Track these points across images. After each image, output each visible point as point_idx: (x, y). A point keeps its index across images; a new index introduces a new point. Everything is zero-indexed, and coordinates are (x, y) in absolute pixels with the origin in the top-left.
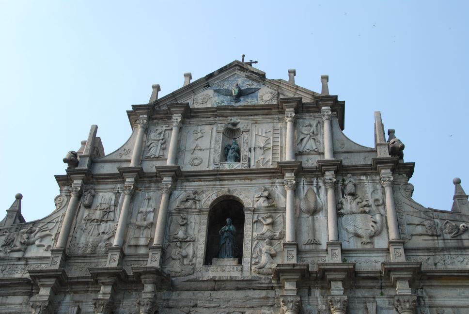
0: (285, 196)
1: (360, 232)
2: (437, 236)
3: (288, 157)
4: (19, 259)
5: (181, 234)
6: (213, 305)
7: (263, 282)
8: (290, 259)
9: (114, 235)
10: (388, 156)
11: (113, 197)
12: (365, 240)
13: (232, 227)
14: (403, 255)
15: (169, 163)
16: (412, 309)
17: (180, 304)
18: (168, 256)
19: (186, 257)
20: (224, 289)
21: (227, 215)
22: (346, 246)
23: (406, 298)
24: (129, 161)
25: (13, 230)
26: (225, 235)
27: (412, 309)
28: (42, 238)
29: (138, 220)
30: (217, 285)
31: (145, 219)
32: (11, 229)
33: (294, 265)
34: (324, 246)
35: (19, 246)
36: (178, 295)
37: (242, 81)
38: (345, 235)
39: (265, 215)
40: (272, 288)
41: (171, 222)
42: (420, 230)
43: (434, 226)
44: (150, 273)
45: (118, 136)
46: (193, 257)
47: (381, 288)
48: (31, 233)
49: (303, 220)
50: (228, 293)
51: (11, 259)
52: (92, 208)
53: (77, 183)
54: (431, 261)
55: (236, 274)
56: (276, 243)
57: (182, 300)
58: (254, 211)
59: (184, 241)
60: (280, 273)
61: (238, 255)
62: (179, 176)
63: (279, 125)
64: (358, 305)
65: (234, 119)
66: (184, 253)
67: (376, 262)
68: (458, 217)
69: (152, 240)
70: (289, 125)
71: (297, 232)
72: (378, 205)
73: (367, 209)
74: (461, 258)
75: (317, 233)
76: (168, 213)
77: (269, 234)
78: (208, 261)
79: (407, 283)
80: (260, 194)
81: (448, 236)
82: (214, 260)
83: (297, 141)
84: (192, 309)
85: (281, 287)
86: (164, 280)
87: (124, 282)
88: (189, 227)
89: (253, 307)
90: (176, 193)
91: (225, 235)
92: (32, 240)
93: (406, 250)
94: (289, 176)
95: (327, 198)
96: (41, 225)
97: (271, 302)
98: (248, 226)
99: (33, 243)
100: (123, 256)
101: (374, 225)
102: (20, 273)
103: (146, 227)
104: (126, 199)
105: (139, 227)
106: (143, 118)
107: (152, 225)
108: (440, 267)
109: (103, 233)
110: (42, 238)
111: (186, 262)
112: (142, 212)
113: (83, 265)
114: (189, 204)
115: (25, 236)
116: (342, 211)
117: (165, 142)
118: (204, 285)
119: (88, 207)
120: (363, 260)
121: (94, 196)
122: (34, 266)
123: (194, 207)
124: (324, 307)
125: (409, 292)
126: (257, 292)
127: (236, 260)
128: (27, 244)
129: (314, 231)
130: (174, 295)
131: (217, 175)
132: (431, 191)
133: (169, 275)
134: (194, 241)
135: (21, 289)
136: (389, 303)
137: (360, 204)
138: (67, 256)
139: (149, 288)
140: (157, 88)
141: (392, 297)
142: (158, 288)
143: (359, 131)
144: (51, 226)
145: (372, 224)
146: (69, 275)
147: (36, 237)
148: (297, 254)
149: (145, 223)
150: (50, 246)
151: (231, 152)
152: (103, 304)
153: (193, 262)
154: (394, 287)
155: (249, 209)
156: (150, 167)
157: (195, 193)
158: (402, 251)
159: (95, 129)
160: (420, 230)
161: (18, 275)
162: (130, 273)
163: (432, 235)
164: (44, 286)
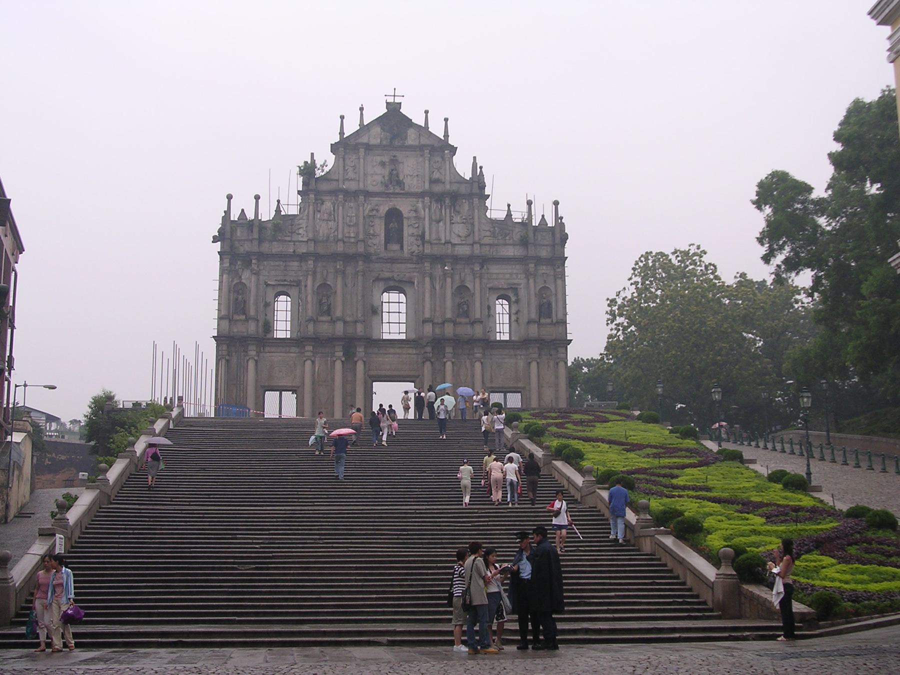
3: (427, 186)
5: (372, 232)
8: (428, 250)
9: (337, 230)
10: (478, 192)
15: (361, 186)
22: (454, 241)
24: (338, 180)
30: (393, 261)
34: (443, 241)
42: (488, 234)
45: (326, 160)
58: (408, 218)
60: (421, 258)
61: (400, 241)
62: (368, 194)
63: (421, 159)
65: (394, 153)
66: (374, 242)
69: (357, 234)
70: (427, 162)
78: (386, 248)
86: (367, 257)
93: (481, 245)
94: (427, 199)
95: (446, 213)
98: (405, 228)
104: (341, 208)
105: (349, 226)
114: (374, 212)
128: (292, 233)
129: (438, 232)
130: (371, 265)
132: (496, 210)
139: (361, 263)
142: (364, 262)
154: (473, 264)
159: (312, 154)
160: (488, 234)
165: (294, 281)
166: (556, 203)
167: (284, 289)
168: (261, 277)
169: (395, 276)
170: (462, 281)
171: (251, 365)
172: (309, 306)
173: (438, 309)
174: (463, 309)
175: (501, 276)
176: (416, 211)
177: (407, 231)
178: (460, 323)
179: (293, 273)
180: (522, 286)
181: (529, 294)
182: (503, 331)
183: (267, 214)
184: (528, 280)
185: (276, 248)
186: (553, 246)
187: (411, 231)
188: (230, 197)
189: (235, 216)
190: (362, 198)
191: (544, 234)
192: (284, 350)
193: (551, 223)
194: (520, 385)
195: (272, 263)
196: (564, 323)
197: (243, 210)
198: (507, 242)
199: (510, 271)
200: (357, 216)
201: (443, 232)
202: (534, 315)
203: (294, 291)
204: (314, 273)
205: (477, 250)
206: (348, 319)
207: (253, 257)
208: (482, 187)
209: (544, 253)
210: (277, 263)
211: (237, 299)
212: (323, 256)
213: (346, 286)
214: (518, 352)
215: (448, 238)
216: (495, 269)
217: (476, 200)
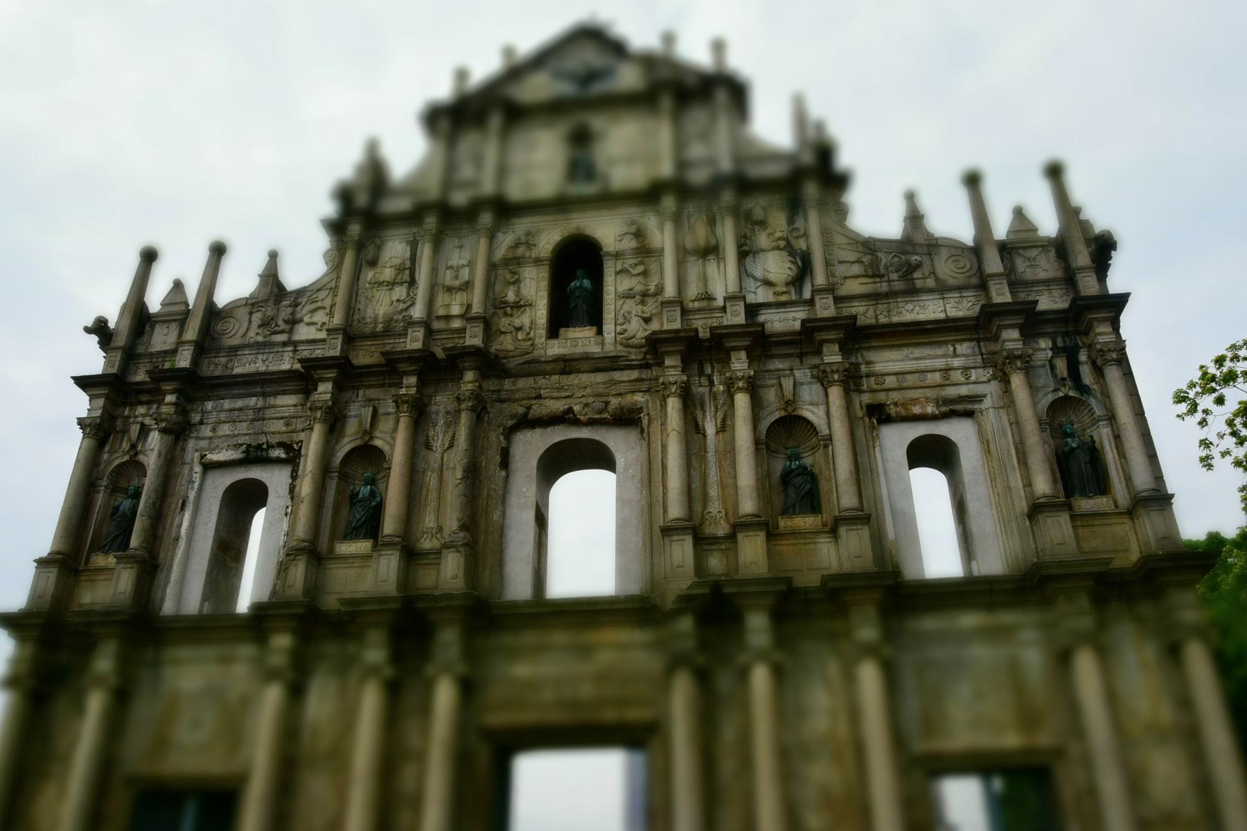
0: (662, 231)
1: (772, 277)
2: (881, 276)
4: (285, 344)
5: (511, 296)
6: (564, 394)
7: (633, 357)
8: (671, 322)
11: (408, 249)
12: (779, 289)
13: (586, 283)
14: (833, 307)
16: (842, 381)
17: (517, 396)
18: (494, 329)
19: (519, 329)
20: (579, 371)
21: (578, 264)
22: (751, 299)
23: (835, 368)
25: (270, 303)
26: (577, 293)
27: (842, 381)
28: (313, 311)
29: (448, 278)
30: (567, 365)
31: (457, 277)
32: (266, 301)
33: (677, 331)
34: (720, 302)
35: (282, 326)
36: (514, 384)
37: (590, 57)
38: (750, 284)
39: (632, 261)
40: (647, 366)
41: (496, 278)
42: (856, 269)
43: (875, 263)
44: (470, 354)
45: (408, 152)
46: (531, 329)
47: (801, 356)
48: (296, 305)
49: (689, 264)
50: (585, 378)
51: (273, 344)
52: (381, 262)
53: (355, 229)
54: (870, 313)
55: (595, 349)
56: (650, 301)
57: (518, 390)
58: (617, 255)
59: (518, 306)
60: (656, 345)
61: (596, 320)
62: (505, 210)
64: (769, 382)
66: (517, 322)
67: (794, 319)
68: (909, 248)
69: (469, 307)
71: (681, 283)
72: (798, 237)
73: (782, 244)
74: (910, 307)
75: (710, 282)
76: (492, 267)
77: (639, 288)
79: (836, 348)
80: (625, 229)
81: (894, 276)
82: (562, 331)
83: (680, 145)
84: (533, 402)
85: (661, 364)
86: (490, 364)
87: (436, 367)
88: (522, 285)
89: (620, 394)
90: (500, 236)
91: (577, 293)
92: (298, 316)
93: (838, 300)
94: (669, 202)
96: (308, 294)
97: (645, 386)
99: (301, 321)
100: (430, 332)
101: (792, 266)
102: (286, 363)
103: (460, 289)
105: (449, 290)
106: (444, 124)
107: (467, 286)
108: (883, 320)
109: (398, 301)
110: (313, 311)
111: (520, 336)
112: (451, 267)
113: (373, 349)
114: (521, 251)
115: (289, 310)
116: (746, 248)
117: (478, 161)
118: (548, 368)
119: (373, 263)
120: (776, 317)
121: (379, 247)
122: (305, 352)
123: (527, 255)
124: (721, 388)
125: (838, 358)
126: (627, 373)
127: (595, 329)
128: (293, 322)
129: (705, 280)
130: (507, 384)
131: (559, 205)
132: (874, 213)
133: (497, 356)
134: (530, 305)
135: (291, 386)
136: (812, 376)
137: (772, 238)
138: (350, 335)
140: (461, 75)
141: (816, 367)
143: (771, 126)
144: (322, 294)
145: (789, 265)
146: (355, 362)
147: (304, 311)
148: (682, 316)
149: (457, 283)
150: (324, 324)
151: (580, 168)
152: (407, 402)
153: (532, 334)
154: (819, 352)
155: (608, 254)
156: (459, 198)
157: (528, 234)
158: (830, 301)
160: (856, 269)
161: (286, 366)
162: (440, 354)
163: (873, 276)
164: (323, 380)
165: (281, 445)
166: (1055, 172)
167: (256, 473)
168: (191, 444)
169: (576, 408)
170: (791, 403)
171: (95, 703)
172: (304, 510)
173: (714, 492)
174: (795, 488)
175: (911, 380)
176: (639, 234)
177: (613, 285)
178: (794, 533)
179: (279, 426)
180: (987, 403)
181: (1016, 423)
182: (938, 555)
183: (237, 285)
184: (1005, 380)
185: (245, 365)
186: (1069, 279)
187: (626, 284)
188: (149, 257)
189: (155, 300)
190: (486, 219)
191: (1033, 253)
192: (210, 651)
193: (1048, 223)
194: (1044, 739)
195: (227, 404)
196: (1160, 499)
197: (178, 286)
198: (919, 284)
199: (939, 363)
200: (471, 264)
201: (722, 279)
202: (1043, 484)
203: (276, 479)
204: (335, 422)
205: (825, 308)
206: (427, 544)
207: (167, 387)
208: (824, 153)
209: (1049, 301)
210: (239, 403)
211: (116, 509)
212: (368, 372)
213: (428, 447)
214: (1008, 617)
215: (733, 288)
216: (888, 362)
217: (811, 190)
